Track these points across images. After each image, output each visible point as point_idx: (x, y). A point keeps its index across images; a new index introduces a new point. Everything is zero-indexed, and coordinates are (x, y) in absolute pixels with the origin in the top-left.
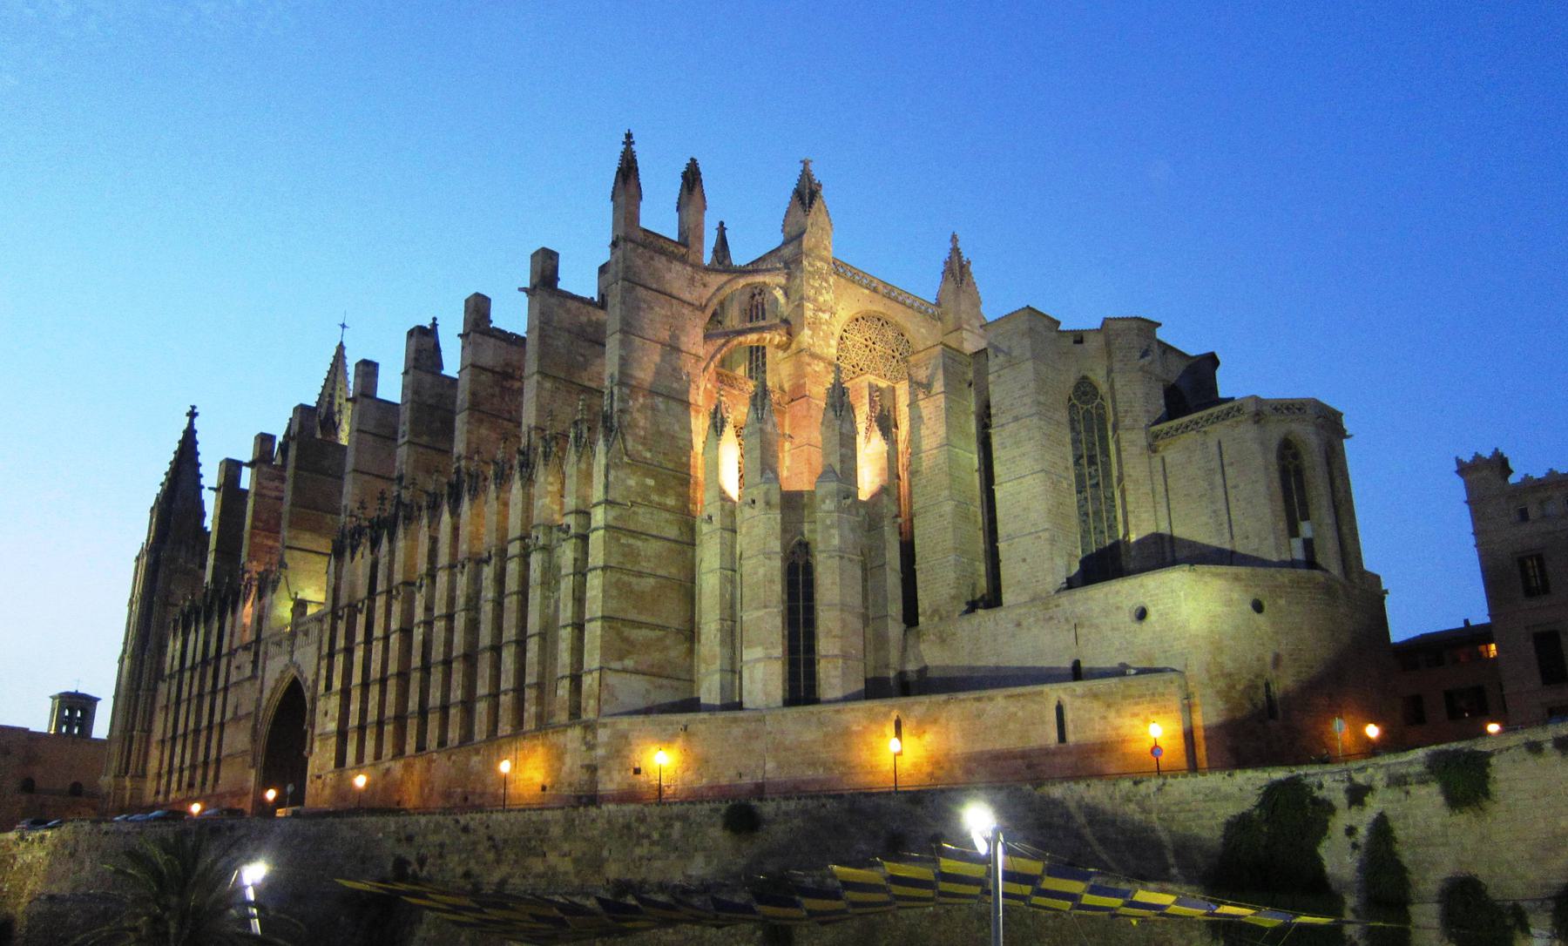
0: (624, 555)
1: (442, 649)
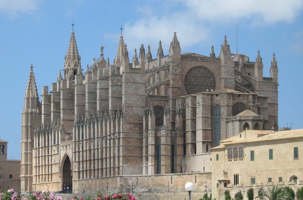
0: (127, 142)
1: (97, 156)
